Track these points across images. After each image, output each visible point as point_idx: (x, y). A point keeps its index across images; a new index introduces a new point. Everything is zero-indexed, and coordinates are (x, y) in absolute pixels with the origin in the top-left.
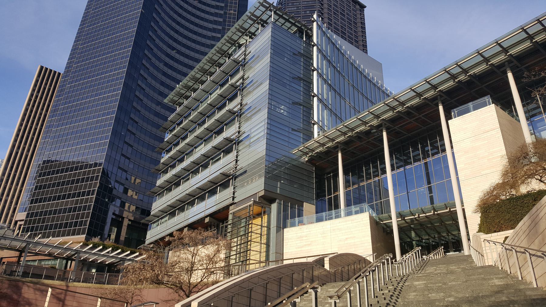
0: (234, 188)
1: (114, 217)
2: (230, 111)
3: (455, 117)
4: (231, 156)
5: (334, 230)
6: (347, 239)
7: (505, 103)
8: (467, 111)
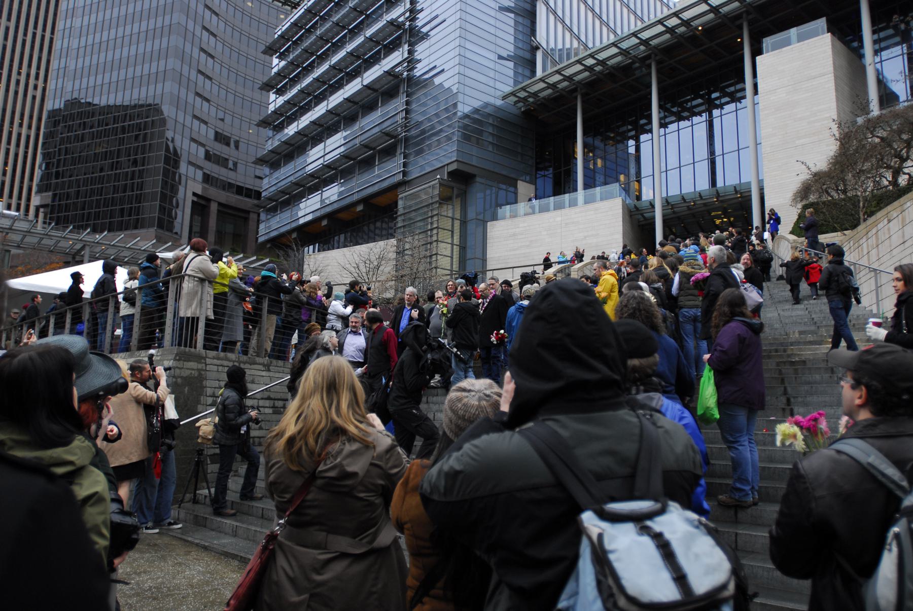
1: (195, 199)
2: (391, 23)
3: (767, 52)
4: (399, 104)
5: (566, 224)
6: (585, 237)
7: (846, 32)
8: (787, 43)
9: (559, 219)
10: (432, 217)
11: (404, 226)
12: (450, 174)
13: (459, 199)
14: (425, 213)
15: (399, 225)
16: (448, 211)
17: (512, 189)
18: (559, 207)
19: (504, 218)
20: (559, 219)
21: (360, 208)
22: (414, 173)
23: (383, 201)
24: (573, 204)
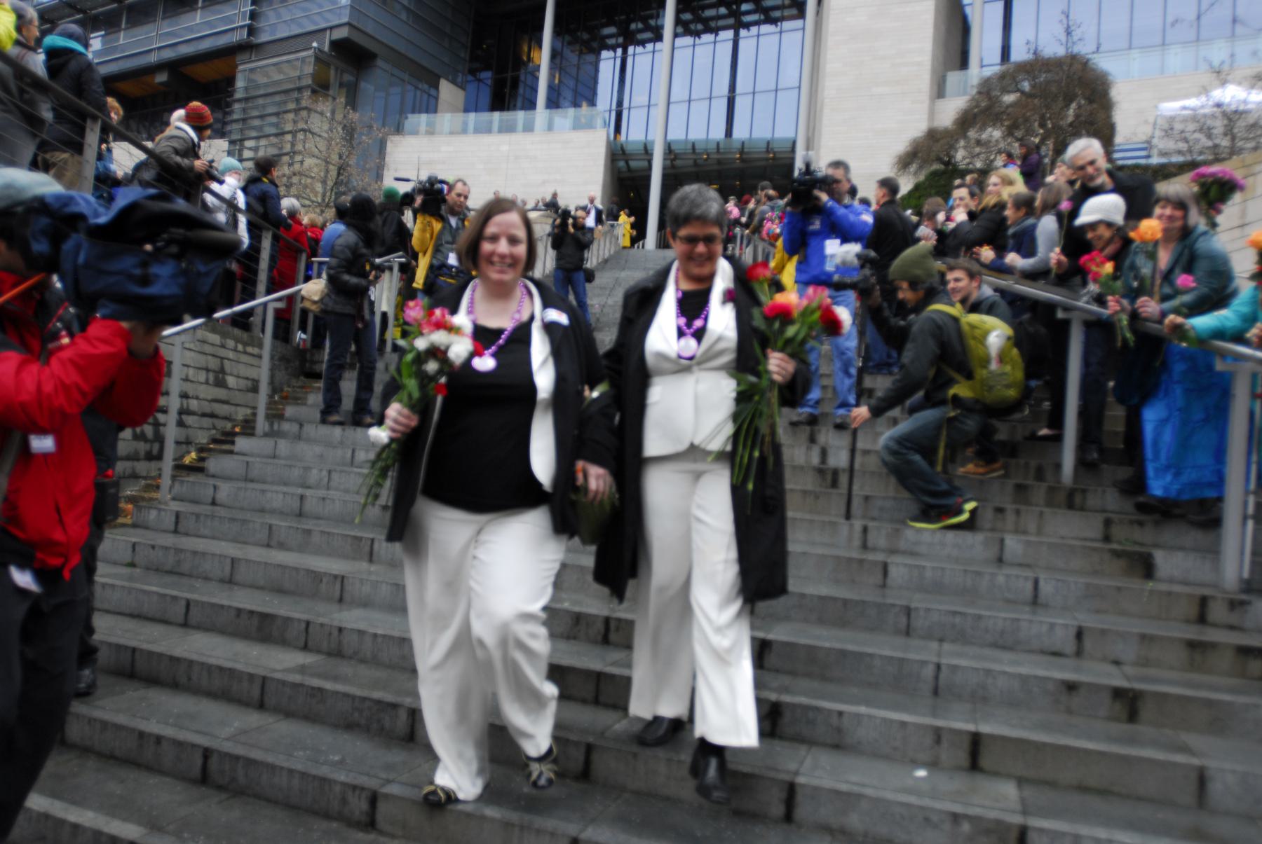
0: (253, 3)
9: (505, 148)
10: (297, 111)
11: (244, 120)
12: (335, 44)
13: (344, 91)
14: (279, 104)
15: (235, 117)
16: (325, 106)
17: (433, 92)
18: (508, 129)
19: (415, 133)
20: (505, 148)
21: (162, 78)
22: (264, 38)
23: (204, 72)
24: (529, 128)
